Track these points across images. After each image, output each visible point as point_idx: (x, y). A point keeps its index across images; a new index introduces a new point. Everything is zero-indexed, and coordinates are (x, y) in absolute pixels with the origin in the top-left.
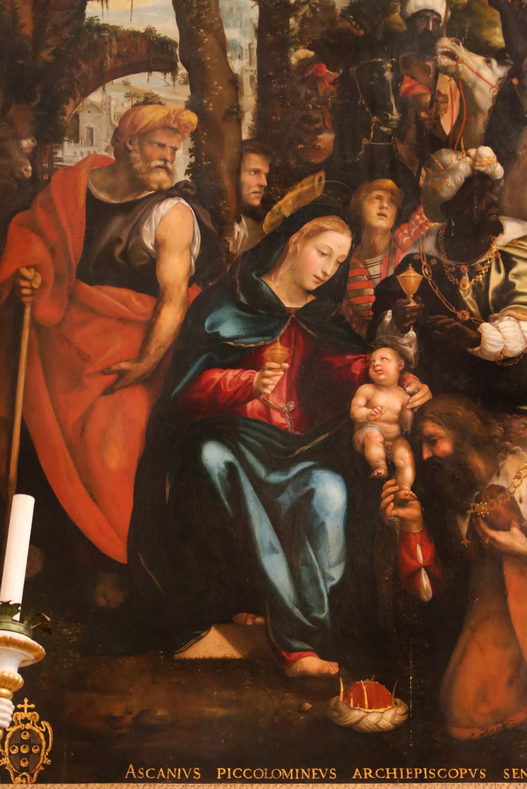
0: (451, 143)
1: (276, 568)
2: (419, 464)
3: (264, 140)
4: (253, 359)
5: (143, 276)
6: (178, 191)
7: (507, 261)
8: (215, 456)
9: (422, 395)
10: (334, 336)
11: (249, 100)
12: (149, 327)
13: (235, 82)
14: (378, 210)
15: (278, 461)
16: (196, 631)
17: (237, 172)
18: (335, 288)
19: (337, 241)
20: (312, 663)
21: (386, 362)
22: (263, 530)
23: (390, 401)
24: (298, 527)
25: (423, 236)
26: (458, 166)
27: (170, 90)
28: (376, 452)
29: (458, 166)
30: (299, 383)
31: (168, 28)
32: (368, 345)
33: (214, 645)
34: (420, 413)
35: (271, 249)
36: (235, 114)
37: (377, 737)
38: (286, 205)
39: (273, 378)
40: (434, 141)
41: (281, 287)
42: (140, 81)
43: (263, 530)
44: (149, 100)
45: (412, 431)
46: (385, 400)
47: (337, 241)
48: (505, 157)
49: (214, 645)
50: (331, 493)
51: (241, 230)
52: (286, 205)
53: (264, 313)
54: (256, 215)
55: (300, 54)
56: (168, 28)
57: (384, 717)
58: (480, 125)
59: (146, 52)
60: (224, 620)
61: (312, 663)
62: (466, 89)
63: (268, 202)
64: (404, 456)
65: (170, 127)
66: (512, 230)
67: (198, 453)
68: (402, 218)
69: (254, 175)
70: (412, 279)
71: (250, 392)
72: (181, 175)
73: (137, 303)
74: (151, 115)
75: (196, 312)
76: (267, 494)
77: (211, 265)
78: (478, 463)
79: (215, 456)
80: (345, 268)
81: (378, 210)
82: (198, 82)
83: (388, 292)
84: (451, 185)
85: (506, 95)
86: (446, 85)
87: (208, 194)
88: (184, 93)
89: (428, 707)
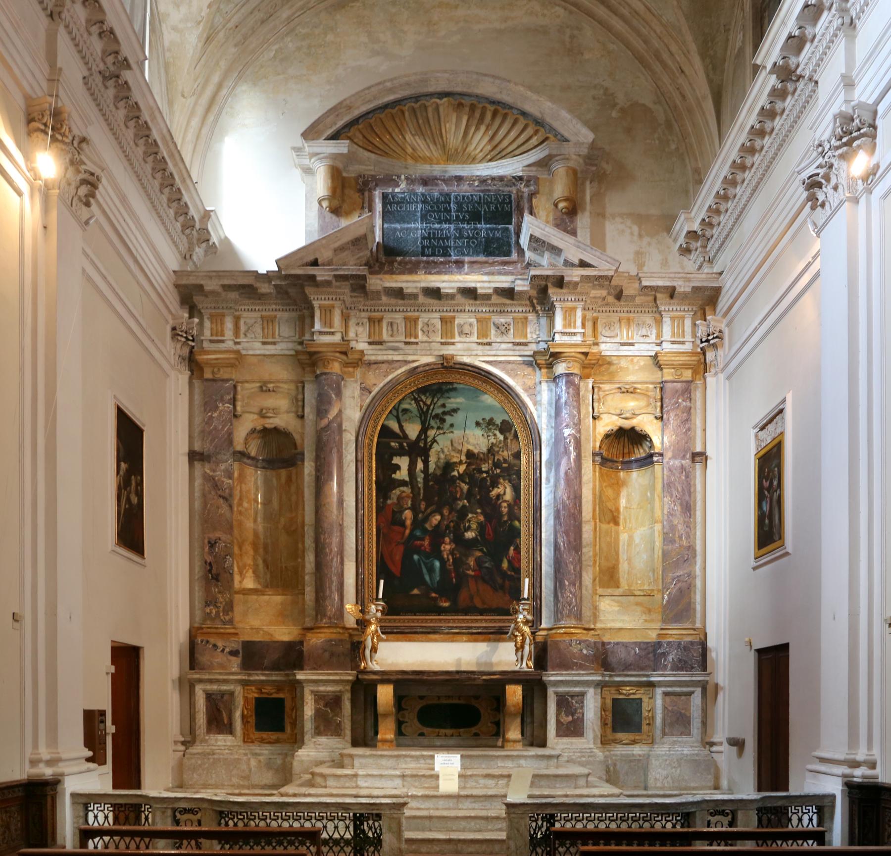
0: (459, 499)
1: (427, 578)
2: (453, 559)
3: (425, 499)
4: (423, 539)
5: (402, 524)
6: (409, 508)
7: (469, 521)
8: (416, 557)
9: (454, 546)
10: (437, 535)
11: (422, 491)
12: (404, 533)
13: (419, 488)
14: (446, 512)
15: (428, 558)
16: (413, 589)
17: (420, 505)
18: (438, 526)
19: (438, 517)
20: (433, 595)
21: (447, 540)
22: (425, 571)
23: (448, 547)
24: (431, 570)
25: (454, 517)
26: (460, 504)
27: (407, 490)
28: (445, 556)
29: (460, 504)
30: (430, 544)
31: (407, 479)
32: (444, 537)
33: (416, 591)
34: (453, 549)
35: (426, 519)
36: (419, 494)
37: (445, 608)
38: (429, 511)
39: (426, 543)
40: (456, 499)
41: (427, 526)
42: (402, 488)
43: (425, 571)
44: (404, 492)
45: (452, 552)
46: (447, 547)
47: (438, 517)
48: (469, 502)
49: (416, 591)
50: (437, 564)
51: (420, 515)
52: (429, 511)
53: (425, 531)
54: (423, 513)
55: (431, 483)
56: (407, 479)
57: (446, 604)
58: (464, 496)
59: (403, 483)
60: (418, 587)
61: (433, 595)
62: (462, 490)
63: (426, 509)
64: (450, 557)
65: (408, 497)
66: (470, 515)
67: (412, 557)
68: (450, 513)
69: (423, 506)
70: (452, 524)
71: (423, 545)
72: (409, 505)
73: (401, 529)
74: (404, 494)
75: (412, 531)
76: (426, 564)
77: (415, 522)
78: (464, 559)
79: (416, 557)
80: (440, 522)
81: (446, 512)
82: (412, 488)
83: (448, 527)
84: (459, 507)
85: (469, 490)
86: (458, 489)
87: (414, 509)
88: (410, 491)
89: (454, 602)
